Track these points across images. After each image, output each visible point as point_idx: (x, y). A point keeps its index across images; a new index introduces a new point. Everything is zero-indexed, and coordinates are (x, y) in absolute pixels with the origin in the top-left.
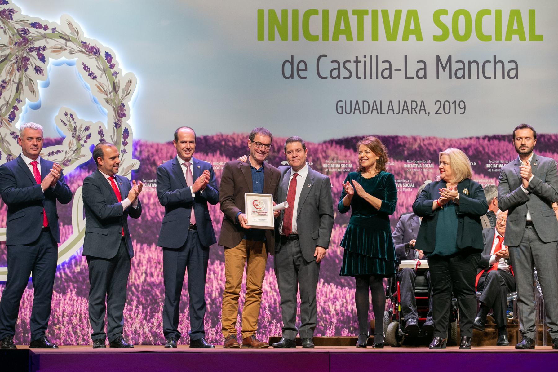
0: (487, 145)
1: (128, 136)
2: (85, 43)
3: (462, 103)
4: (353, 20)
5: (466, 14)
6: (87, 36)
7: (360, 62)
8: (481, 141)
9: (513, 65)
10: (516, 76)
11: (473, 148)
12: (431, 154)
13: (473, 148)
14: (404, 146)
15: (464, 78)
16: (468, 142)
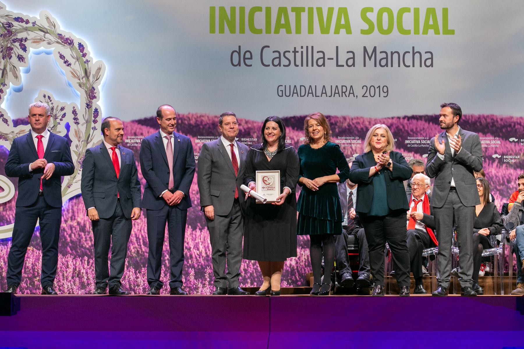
0: (407, 124)
1: (98, 115)
2: (61, 35)
3: (385, 88)
4: (292, 16)
5: (389, 11)
6: (62, 29)
7: (298, 52)
8: (401, 120)
9: (429, 55)
10: (432, 65)
11: (394, 126)
12: (358, 131)
13: (394, 126)
14: (336, 124)
15: (387, 66)
16: (390, 121)
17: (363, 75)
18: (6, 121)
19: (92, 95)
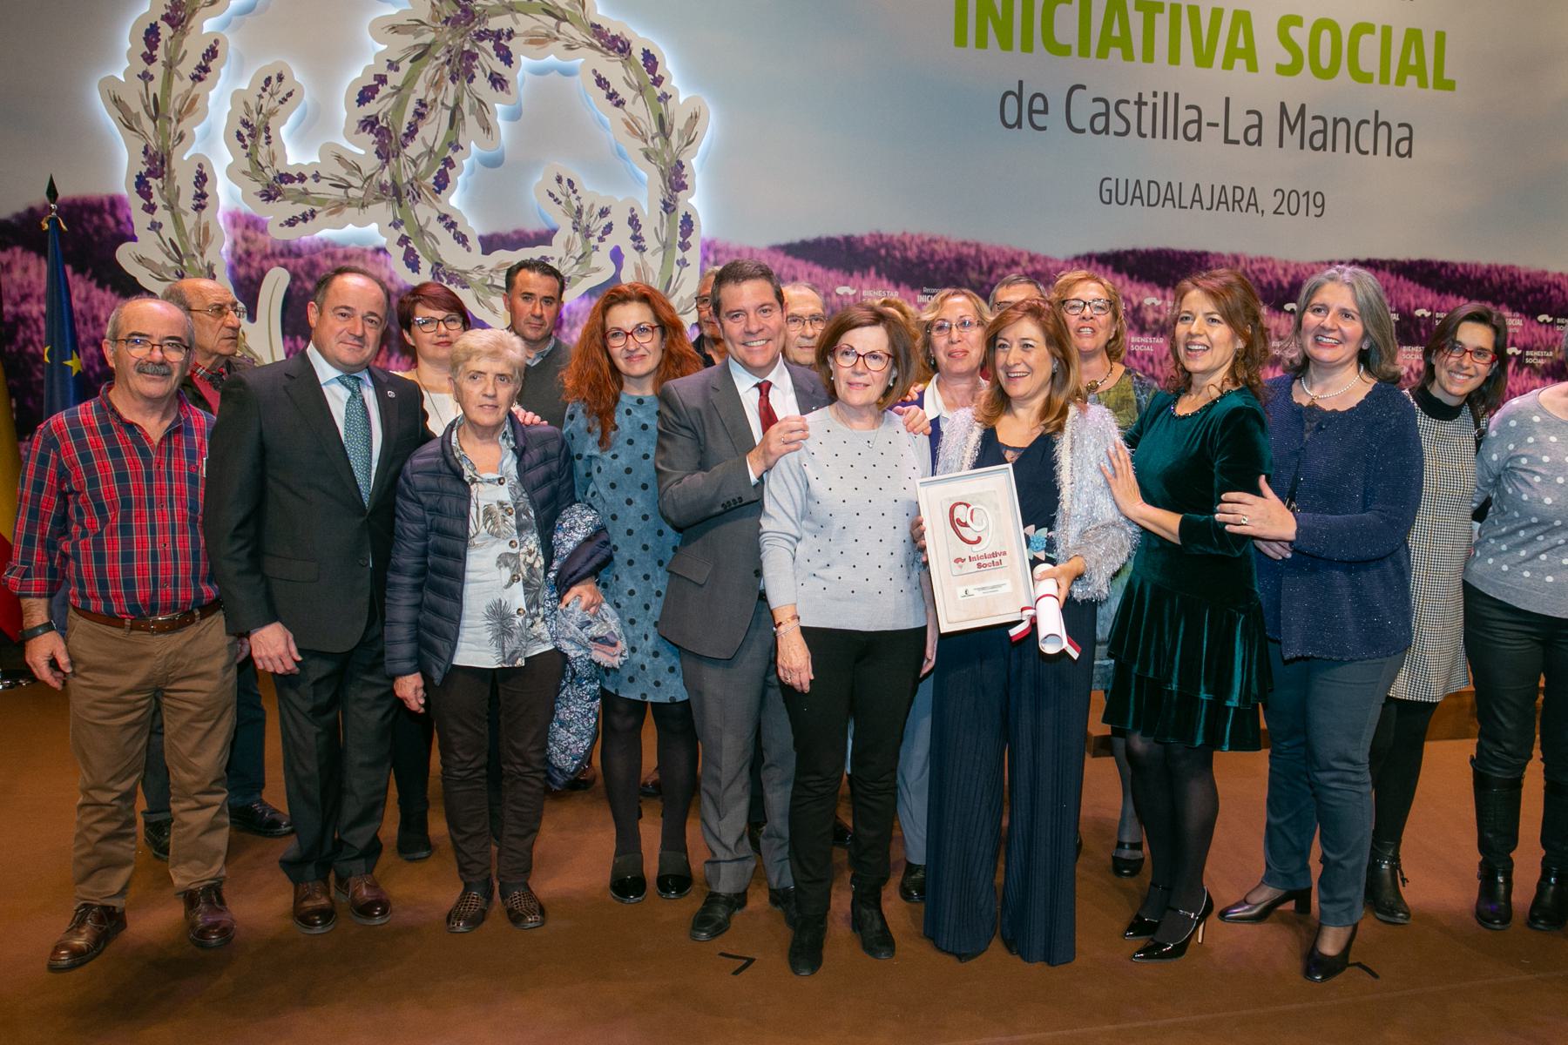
2: (599, 27)
3: (1319, 197)
9: (1405, 132)
10: (1409, 153)
17: (1275, 166)
18: (462, 239)
19: (675, 180)
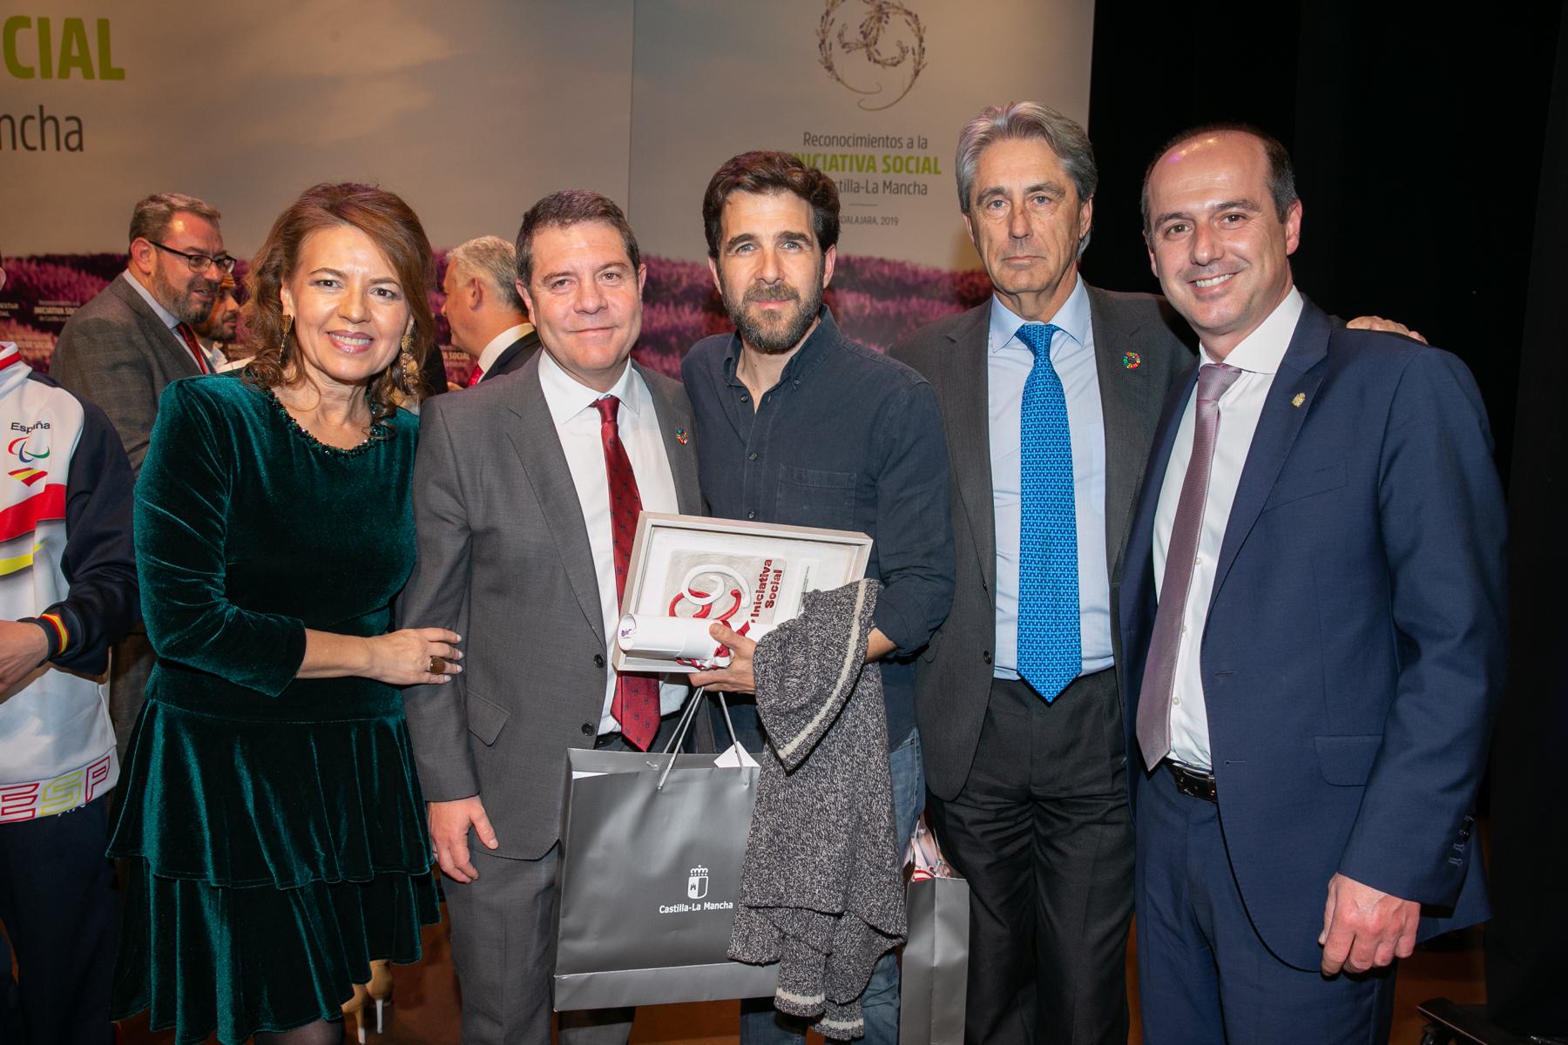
8: (25, 265)
9: (74, 126)
10: (80, 146)
